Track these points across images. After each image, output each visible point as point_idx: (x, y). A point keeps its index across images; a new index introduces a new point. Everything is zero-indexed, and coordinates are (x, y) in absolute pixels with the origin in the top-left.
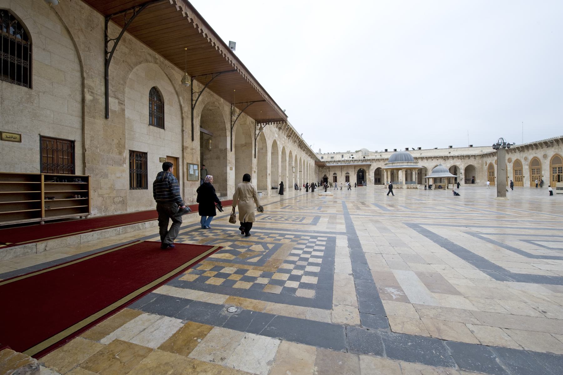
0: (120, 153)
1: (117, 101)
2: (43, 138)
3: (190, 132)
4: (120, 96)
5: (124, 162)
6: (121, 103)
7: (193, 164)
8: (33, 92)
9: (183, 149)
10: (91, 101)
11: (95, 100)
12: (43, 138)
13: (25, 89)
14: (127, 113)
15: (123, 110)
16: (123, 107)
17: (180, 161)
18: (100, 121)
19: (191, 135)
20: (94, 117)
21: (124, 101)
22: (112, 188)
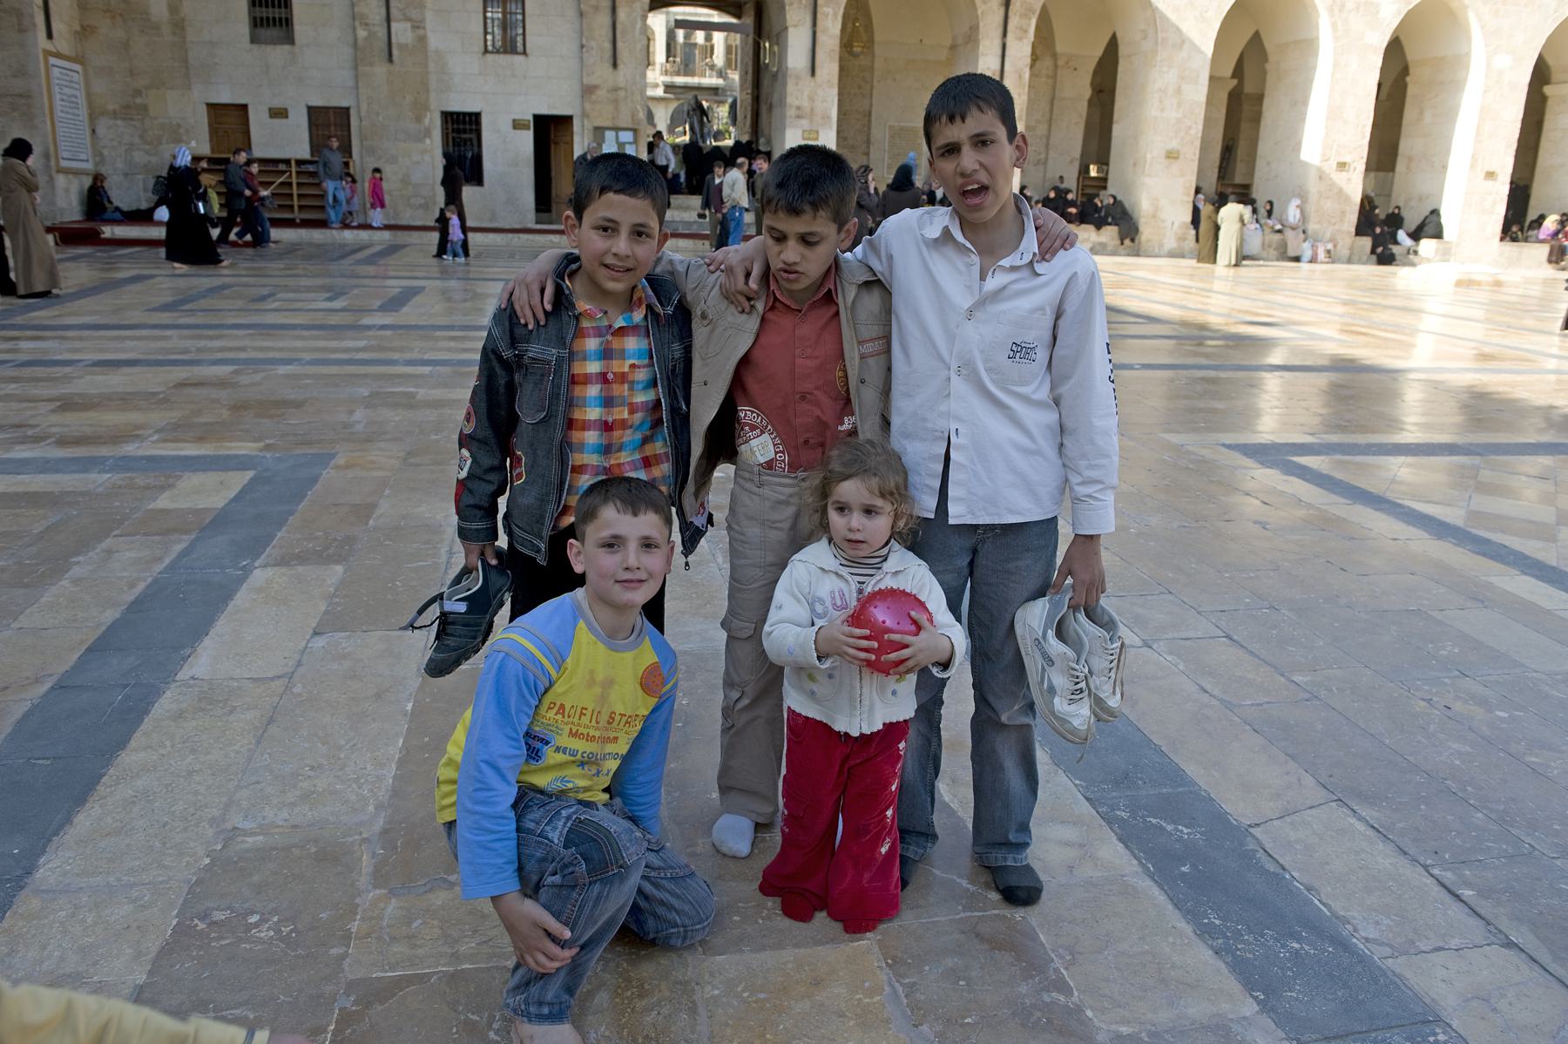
0: (419, 119)
1: (408, 25)
2: (310, 109)
3: (608, 46)
4: (414, 14)
5: (428, 133)
6: (418, 25)
7: (617, 129)
8: (296, 49)
9: (588, 91)
10: (366, 39)
11: (371, 35)
12: (310, 109)
13: (287, 47)
14: (434, 41)
15: (422, 40)
16: (421, 32)
17: (576, 125)
18: (380, 70)
19: (608, 53)
20: (371, 64)
21: (423, 21)
22: (405, 181)
